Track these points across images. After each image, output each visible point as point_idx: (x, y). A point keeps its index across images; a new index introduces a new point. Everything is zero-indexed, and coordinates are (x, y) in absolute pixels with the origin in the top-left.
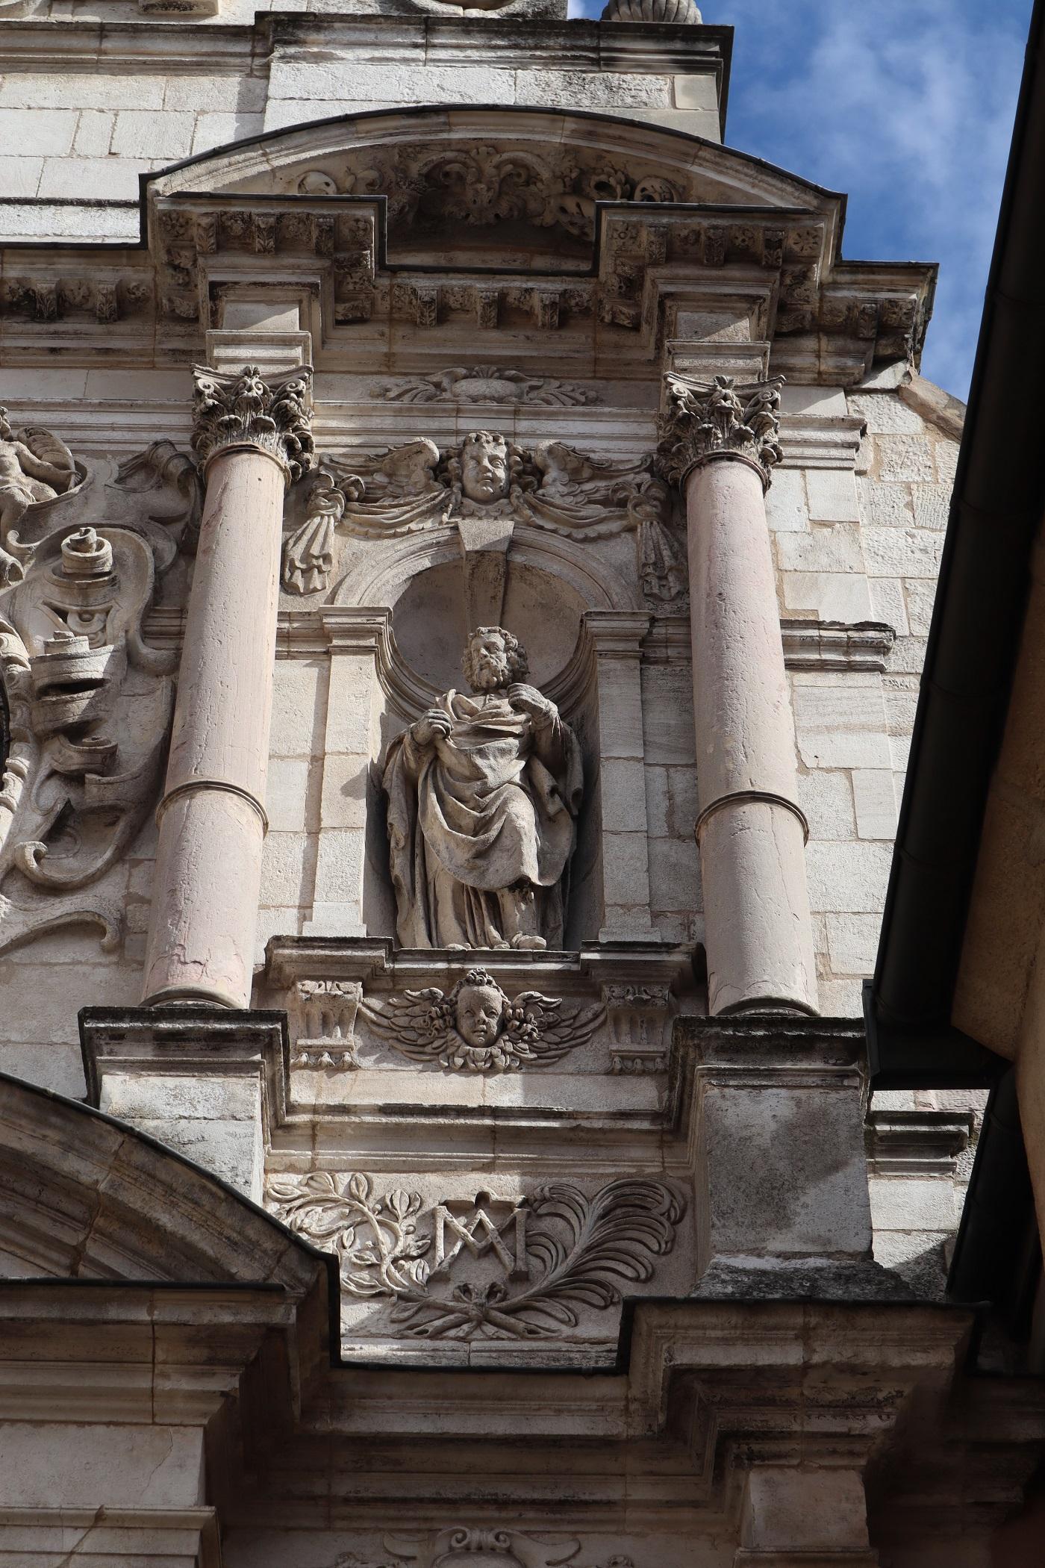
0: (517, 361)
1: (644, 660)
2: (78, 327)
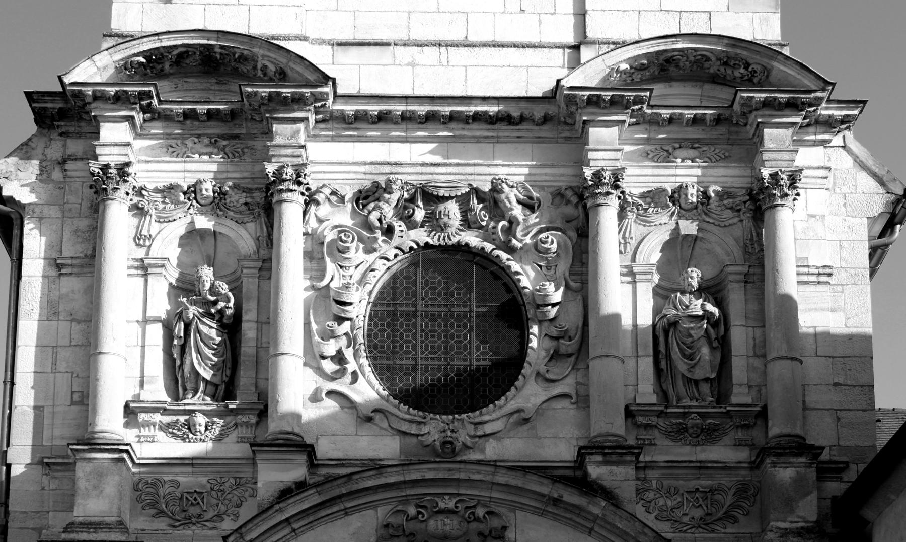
0: (698, 140)
1: (746, 282)
2: (528, 127)
